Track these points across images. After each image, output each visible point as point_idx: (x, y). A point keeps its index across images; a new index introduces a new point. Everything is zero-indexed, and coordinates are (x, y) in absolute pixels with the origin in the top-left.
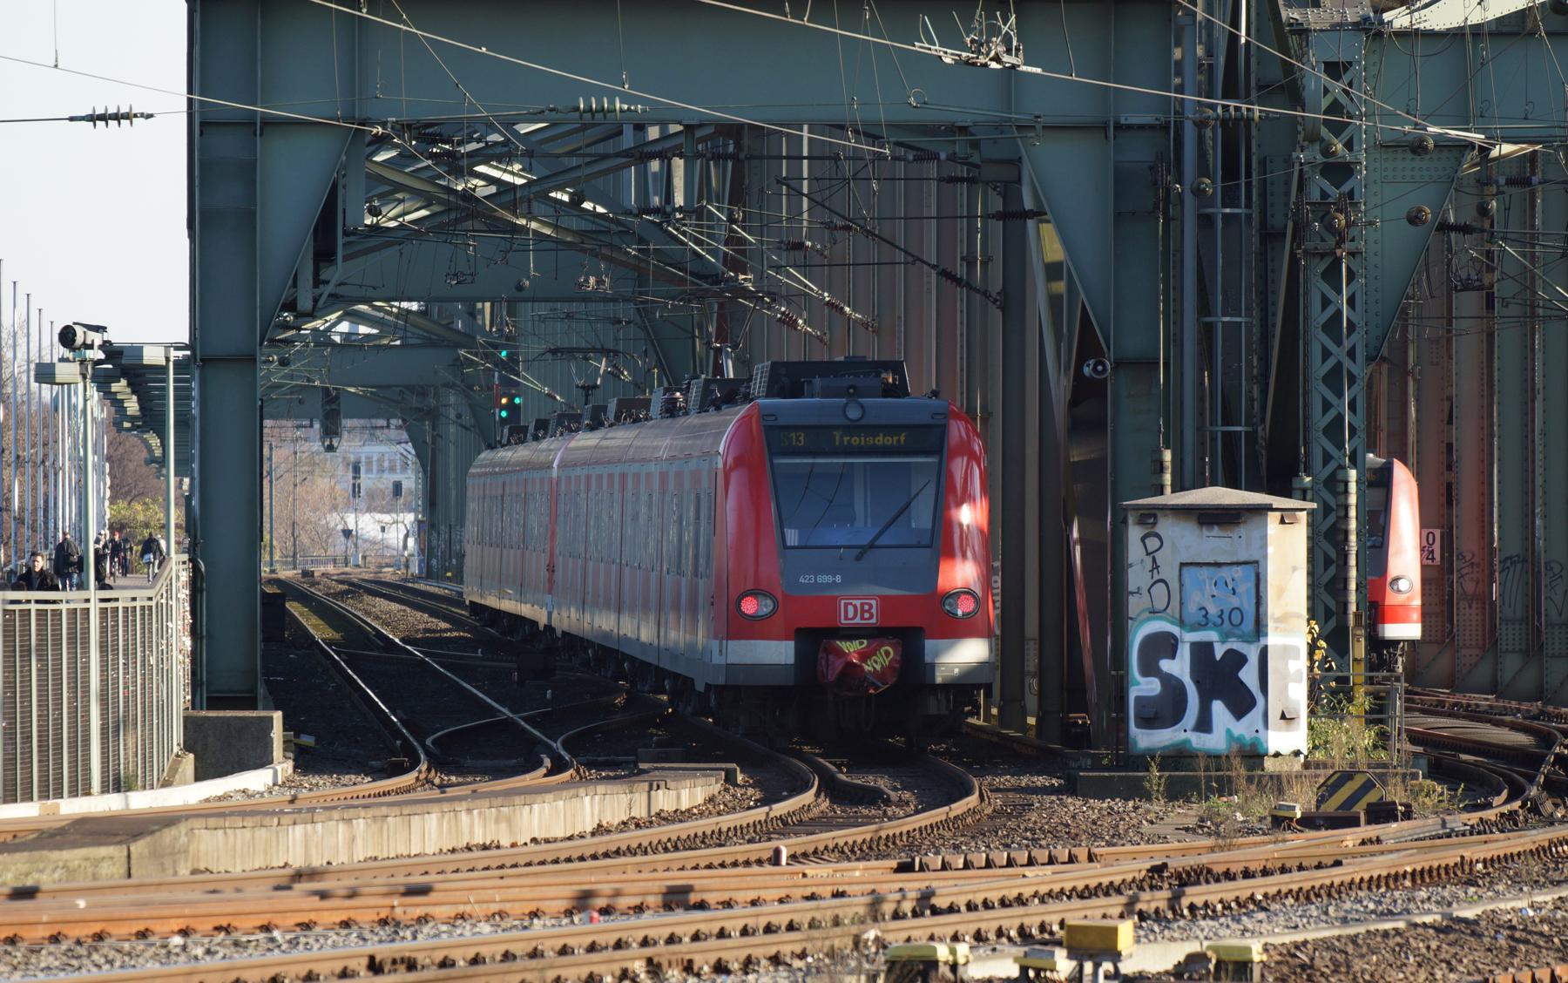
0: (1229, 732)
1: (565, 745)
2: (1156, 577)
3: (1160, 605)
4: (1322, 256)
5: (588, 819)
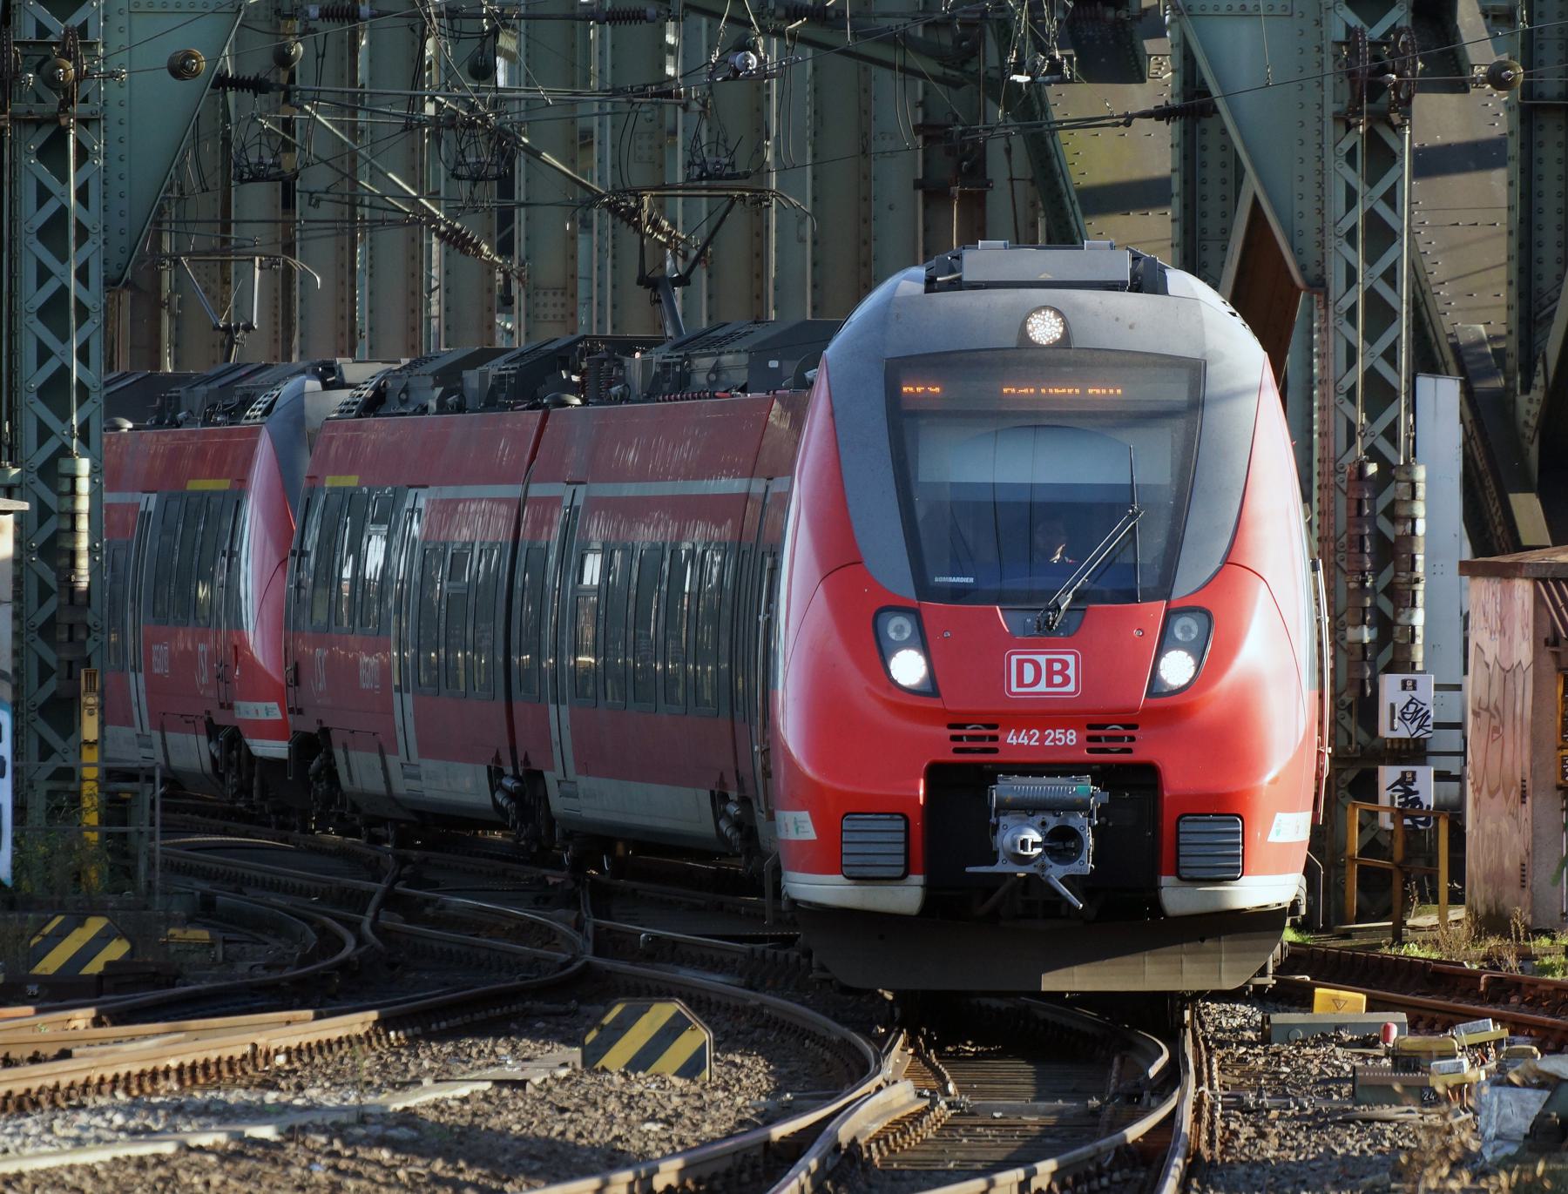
4: (39, 124)
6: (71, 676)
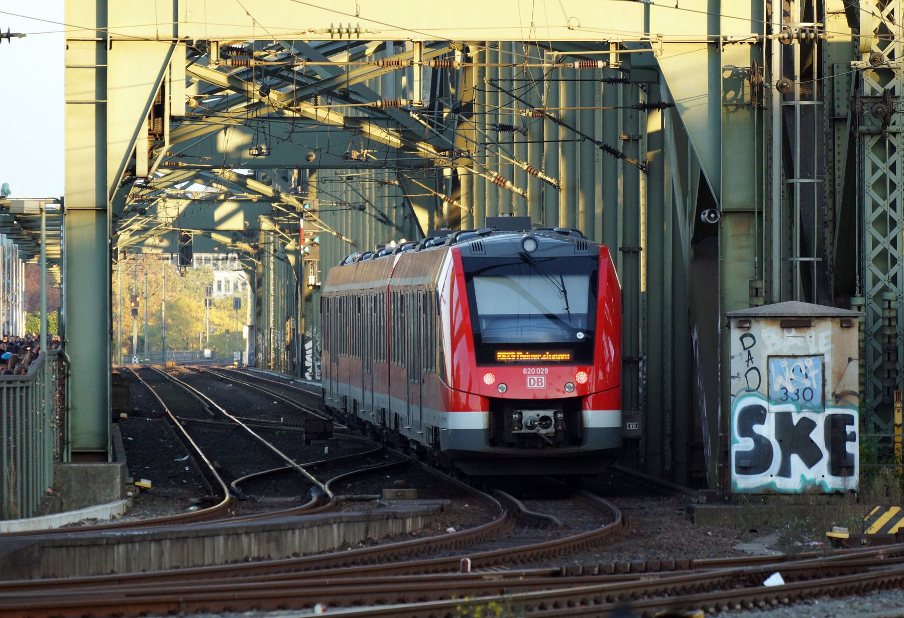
0: (802, 476)
1: (330, 488)
2: (751, 366)
3: (753, 386)
5: (336, 539)
6: (889, 394)
